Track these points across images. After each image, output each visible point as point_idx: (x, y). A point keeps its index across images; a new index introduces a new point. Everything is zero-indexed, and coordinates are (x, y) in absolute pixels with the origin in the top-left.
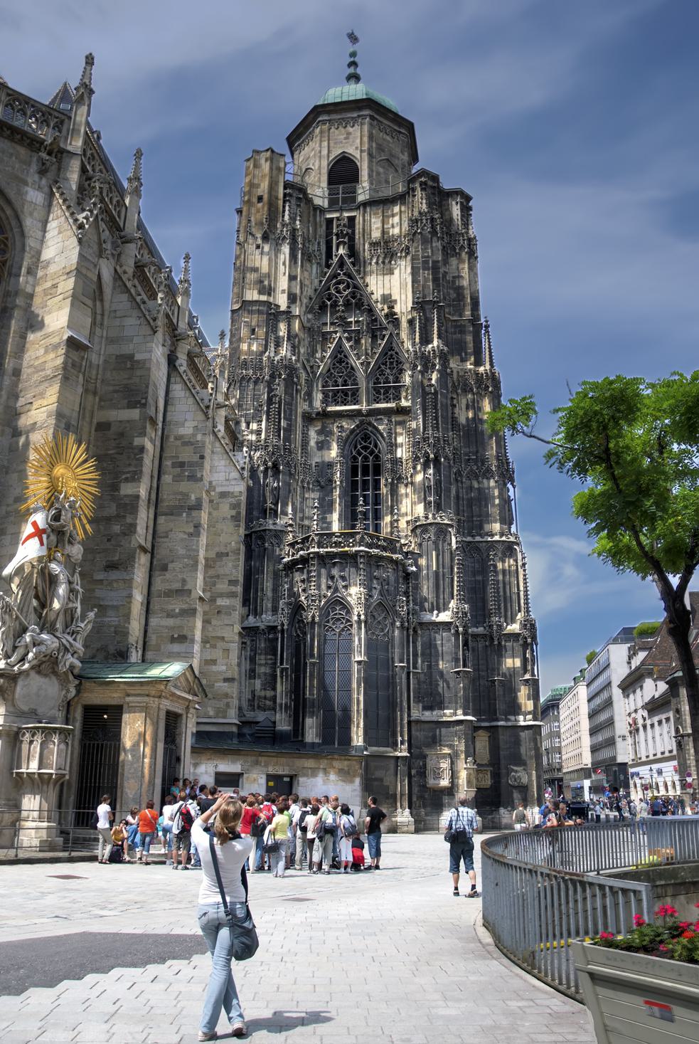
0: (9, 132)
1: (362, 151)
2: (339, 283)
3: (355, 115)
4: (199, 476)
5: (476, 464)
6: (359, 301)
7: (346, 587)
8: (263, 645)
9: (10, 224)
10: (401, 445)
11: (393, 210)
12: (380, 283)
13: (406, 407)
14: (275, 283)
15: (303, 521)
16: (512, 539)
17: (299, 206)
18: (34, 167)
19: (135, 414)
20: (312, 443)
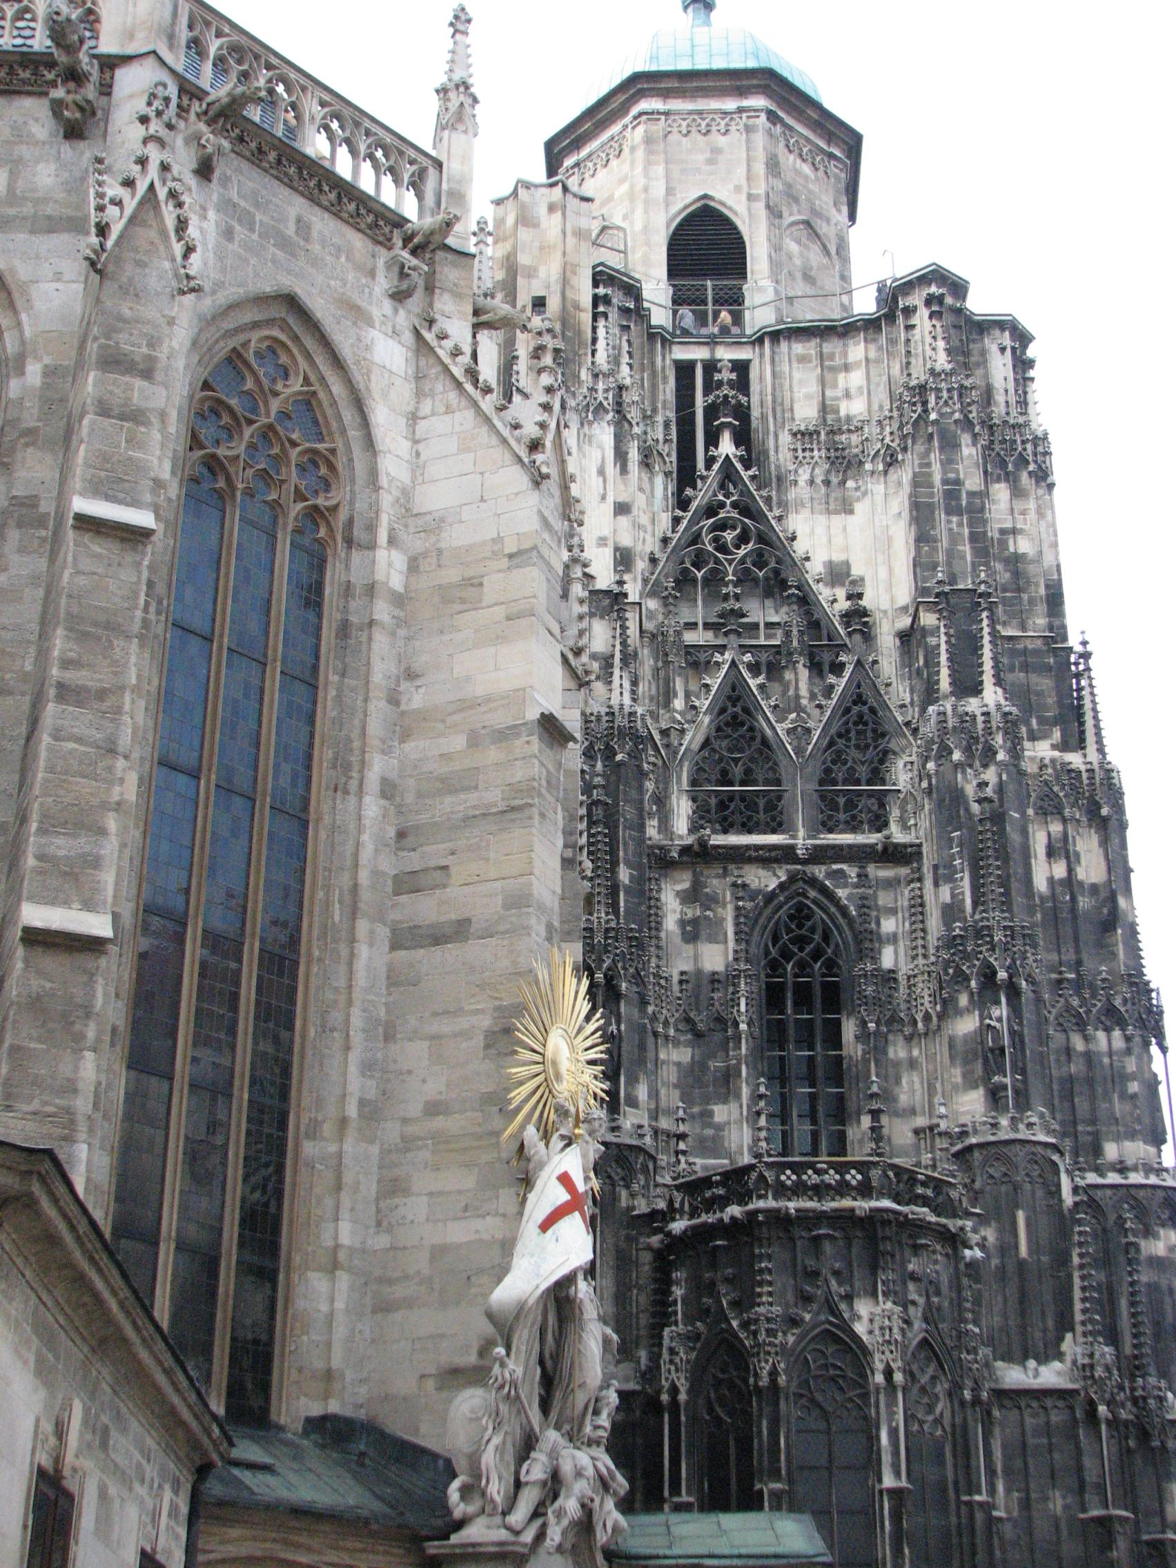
0: (333, 196)
1: (750, 197)
2: (723, 526)
5: (1079, 995)
7: (849, 1298)
9: (339, 417)
10: (893, 939)
11: (845, 354)
12: (820, 530)
13: (905, 846)
15: (656, 1119)
18: (383, 282)
20: (670, 923)
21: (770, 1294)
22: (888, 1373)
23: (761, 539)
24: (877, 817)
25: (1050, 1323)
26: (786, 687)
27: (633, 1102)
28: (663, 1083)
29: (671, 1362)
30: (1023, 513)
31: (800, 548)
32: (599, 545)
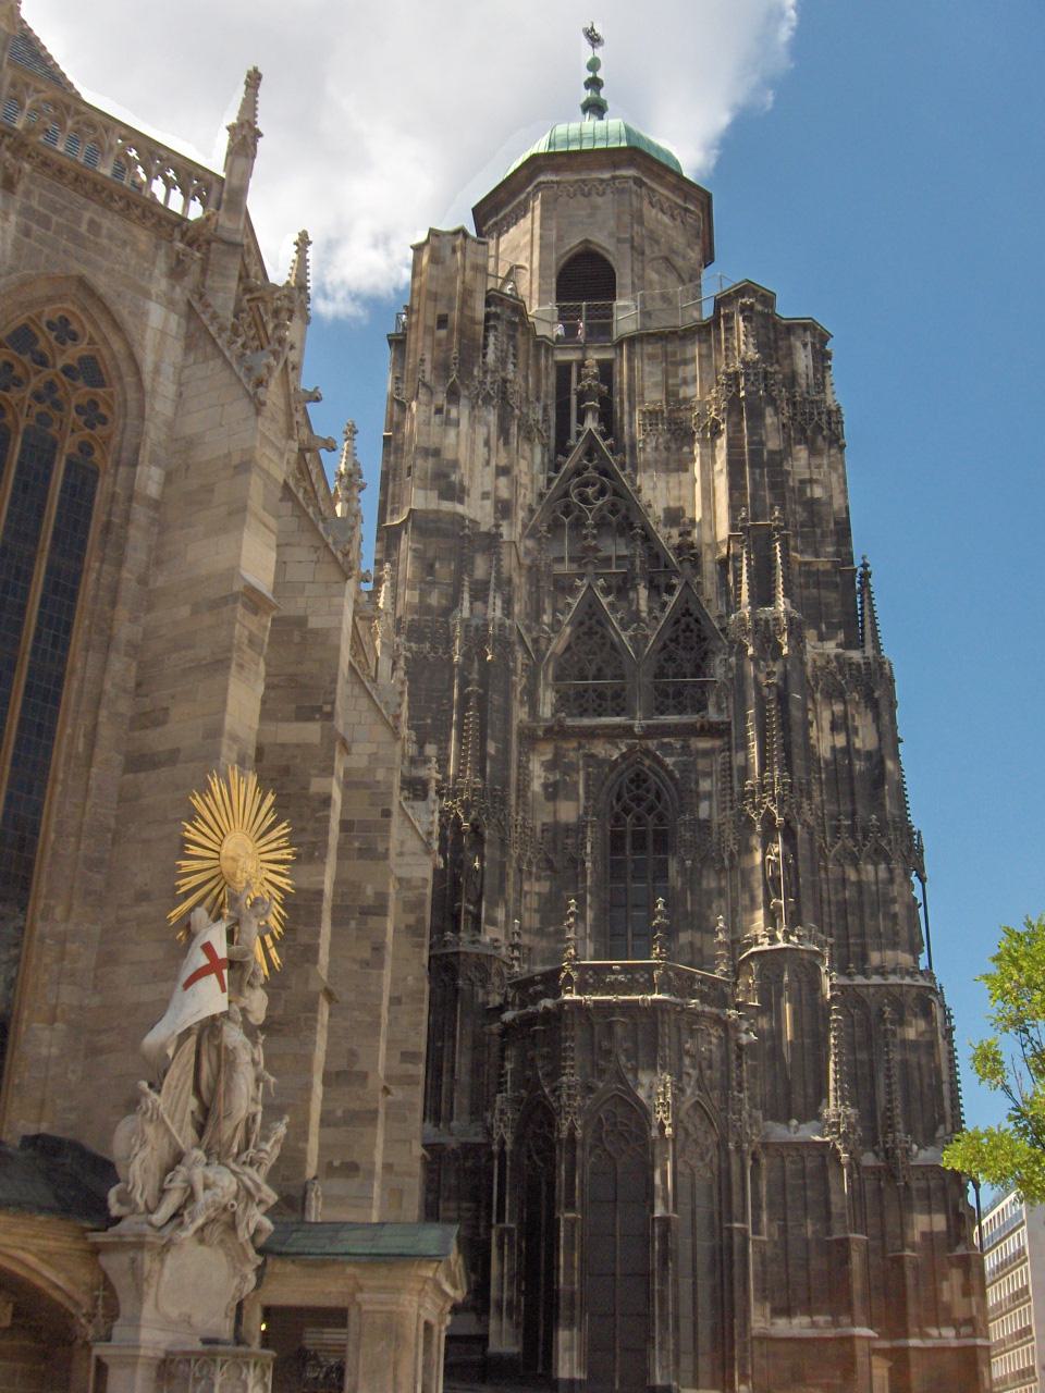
1: (619, 240)
2: (586, 485)
3: (606, 175)
4: (381, 848)
6: (626, 517)
7: (635, 1071)
8: (453, 1181)
9: (118, 368)
10: (709, 796)
12: (661, 485)
13: (718, 724)
14: (471, 478)
16: (922, 982)
17: (512, 337)
18: (161, 266)
19: (311, 732)
20: (536, 786)
21: (572, 1067)
22: (662, 1127)
23: (616, 493)
24: (699, 702)
25: (810, 1091)
26: (630, 603)
27: (493, 922)
28: (527, 909)
29: (501, 1120)
30: (819, 467)
31: (647, 495)
32: (483, 498)
